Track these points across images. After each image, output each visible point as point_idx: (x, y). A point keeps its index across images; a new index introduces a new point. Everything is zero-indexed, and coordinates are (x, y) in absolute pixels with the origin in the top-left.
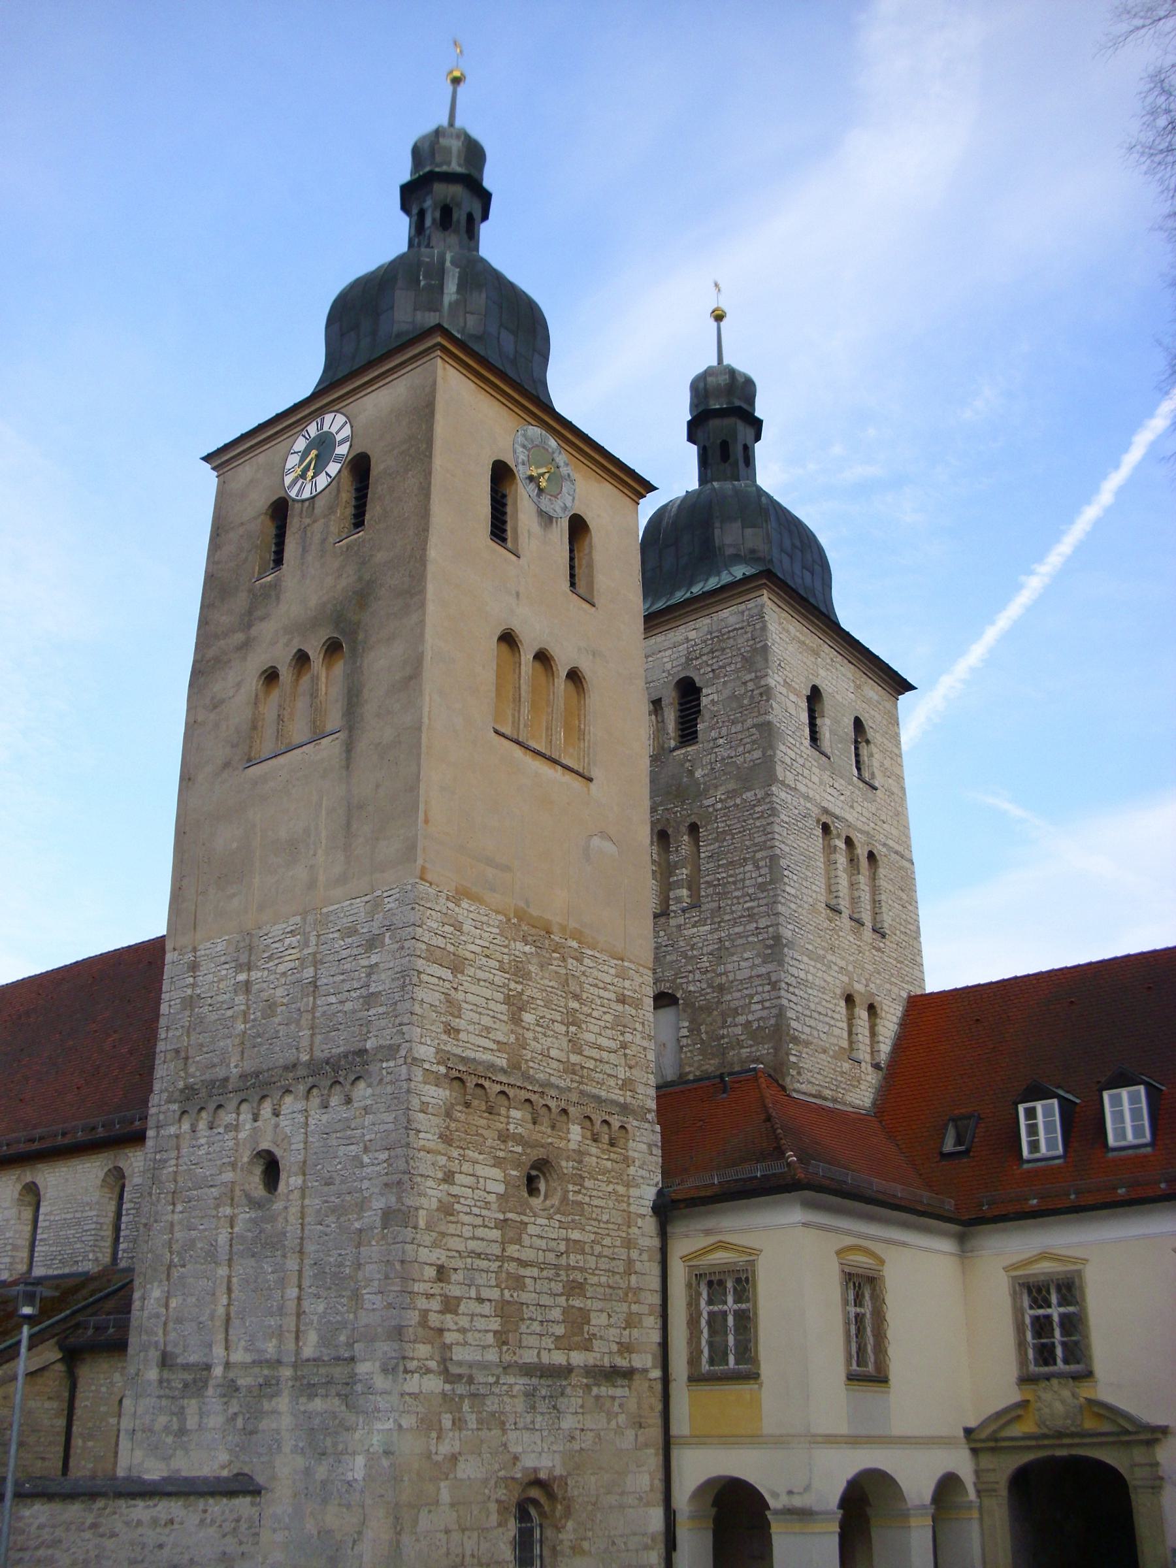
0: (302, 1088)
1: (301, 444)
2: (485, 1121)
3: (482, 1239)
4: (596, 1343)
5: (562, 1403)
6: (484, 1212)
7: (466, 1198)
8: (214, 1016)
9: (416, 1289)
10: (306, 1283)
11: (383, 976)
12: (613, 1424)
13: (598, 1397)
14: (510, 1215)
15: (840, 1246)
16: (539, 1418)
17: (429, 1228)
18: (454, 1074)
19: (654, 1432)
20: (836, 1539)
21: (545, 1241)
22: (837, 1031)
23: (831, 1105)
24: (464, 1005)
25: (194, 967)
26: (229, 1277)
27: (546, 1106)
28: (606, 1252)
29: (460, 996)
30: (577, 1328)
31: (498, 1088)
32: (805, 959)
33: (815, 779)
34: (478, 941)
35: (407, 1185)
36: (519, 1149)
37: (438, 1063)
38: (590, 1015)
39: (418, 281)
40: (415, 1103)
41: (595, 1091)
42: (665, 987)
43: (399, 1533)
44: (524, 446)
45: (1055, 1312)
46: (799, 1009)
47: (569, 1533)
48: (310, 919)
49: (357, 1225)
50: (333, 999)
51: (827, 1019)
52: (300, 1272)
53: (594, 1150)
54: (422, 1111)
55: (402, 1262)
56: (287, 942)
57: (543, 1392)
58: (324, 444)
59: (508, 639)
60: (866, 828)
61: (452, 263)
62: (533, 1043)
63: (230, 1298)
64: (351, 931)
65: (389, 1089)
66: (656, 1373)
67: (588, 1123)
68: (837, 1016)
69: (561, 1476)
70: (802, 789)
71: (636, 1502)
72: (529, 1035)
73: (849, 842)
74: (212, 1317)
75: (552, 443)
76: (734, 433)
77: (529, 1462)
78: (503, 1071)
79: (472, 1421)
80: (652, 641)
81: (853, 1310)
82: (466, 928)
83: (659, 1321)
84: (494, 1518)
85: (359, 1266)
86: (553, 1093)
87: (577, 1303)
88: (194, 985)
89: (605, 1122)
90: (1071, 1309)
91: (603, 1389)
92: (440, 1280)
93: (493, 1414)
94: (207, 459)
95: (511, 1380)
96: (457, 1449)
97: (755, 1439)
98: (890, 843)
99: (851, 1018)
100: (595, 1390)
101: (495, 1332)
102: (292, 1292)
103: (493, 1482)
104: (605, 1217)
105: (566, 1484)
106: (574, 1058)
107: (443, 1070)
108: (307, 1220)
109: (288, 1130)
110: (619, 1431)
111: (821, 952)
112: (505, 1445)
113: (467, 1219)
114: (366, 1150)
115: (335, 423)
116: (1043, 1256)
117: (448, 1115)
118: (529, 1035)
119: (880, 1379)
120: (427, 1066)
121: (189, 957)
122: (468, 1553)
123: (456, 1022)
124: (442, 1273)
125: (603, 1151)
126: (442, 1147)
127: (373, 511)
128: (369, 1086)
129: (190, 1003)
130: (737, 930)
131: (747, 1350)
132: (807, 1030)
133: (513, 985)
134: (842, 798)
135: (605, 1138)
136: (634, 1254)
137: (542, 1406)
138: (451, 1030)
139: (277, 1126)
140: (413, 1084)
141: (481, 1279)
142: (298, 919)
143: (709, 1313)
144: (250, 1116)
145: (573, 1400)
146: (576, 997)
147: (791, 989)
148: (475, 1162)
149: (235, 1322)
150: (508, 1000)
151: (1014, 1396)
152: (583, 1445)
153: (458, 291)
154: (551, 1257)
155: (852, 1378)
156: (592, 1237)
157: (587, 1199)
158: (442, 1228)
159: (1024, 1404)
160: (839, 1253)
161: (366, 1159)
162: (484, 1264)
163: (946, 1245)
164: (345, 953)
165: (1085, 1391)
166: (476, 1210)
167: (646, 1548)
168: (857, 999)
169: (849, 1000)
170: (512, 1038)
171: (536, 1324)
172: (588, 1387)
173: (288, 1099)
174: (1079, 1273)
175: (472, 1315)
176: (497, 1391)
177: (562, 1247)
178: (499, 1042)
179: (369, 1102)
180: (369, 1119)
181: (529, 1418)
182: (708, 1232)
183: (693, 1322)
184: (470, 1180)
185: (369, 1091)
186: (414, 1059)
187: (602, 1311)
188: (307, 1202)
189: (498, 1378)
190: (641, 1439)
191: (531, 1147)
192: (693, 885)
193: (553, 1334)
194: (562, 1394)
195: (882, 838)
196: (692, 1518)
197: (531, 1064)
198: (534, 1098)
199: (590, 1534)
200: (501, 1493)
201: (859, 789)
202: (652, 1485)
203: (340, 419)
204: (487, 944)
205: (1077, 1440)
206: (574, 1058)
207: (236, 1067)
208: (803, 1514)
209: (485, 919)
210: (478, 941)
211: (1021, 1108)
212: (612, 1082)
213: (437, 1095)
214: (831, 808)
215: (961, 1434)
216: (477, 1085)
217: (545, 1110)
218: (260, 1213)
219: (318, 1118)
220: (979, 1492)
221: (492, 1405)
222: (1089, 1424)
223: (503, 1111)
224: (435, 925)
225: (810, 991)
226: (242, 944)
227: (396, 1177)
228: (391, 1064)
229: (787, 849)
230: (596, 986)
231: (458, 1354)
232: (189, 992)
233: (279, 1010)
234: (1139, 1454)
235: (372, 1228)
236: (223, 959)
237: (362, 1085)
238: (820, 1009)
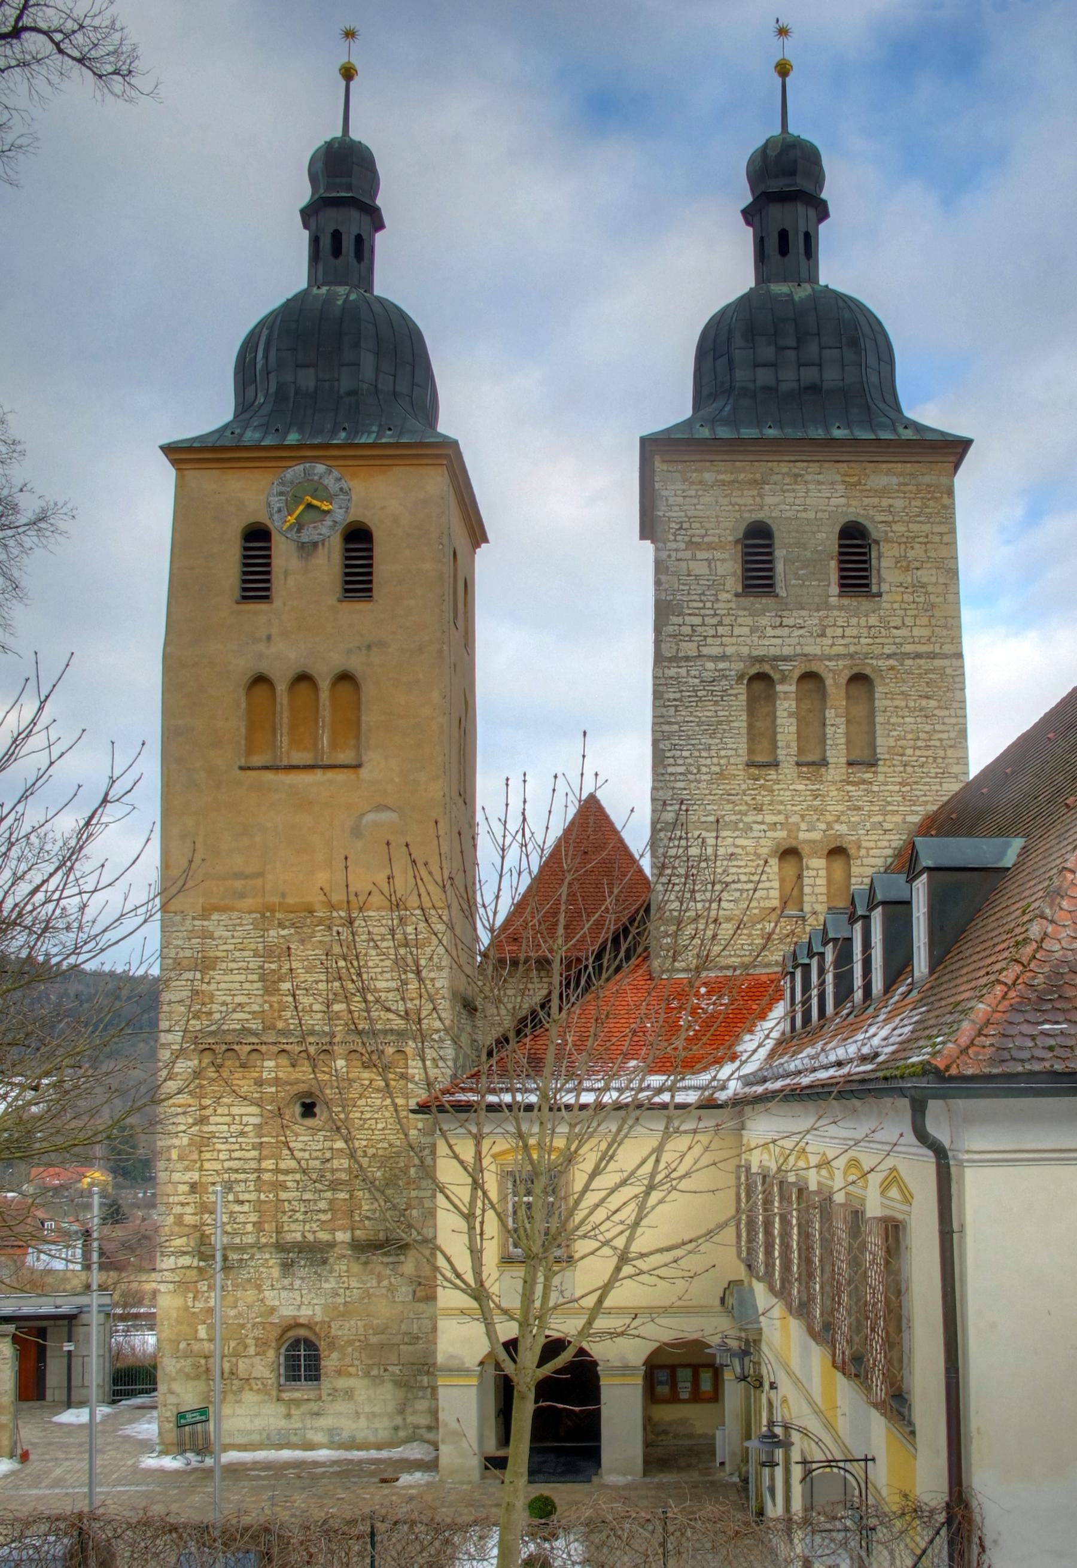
2: (240, 1075)
3: (240, 1159)
6: (240, 1140)
7: (221, 1133)
9: (171, 1201)
12: (385, 1283)
17: (181, 1158)
21: (307, 1153)
36: (273, 1089)
51: (739, 886)
69: (323, 1322)
77: (288, 1311)
82: (216, 935)
84: (252, 1350)
92: (195, 1193)
93: (249, 1280)
98: (908, 648)
101: (254, 1224)
103: (249, 1326)
104: (380, 1126)
105: (330, 1327)
112: (262, 1300)
113: (223, 1147)
124: (194, 1187)
150: (262, 979)
152: (348, 1299)
156: (364, 1143)
162: (242, 1176)
166: (233, 1140)
170: (266, 1007)
171: (298, 1214)
178: (254, 1012)
181: (286, 1282)
184: (228, 1119)
193: (318, 1220)
197: (291, 1021)
198: (288, 1047)
223: (259, 1063)
224: (180, 942)
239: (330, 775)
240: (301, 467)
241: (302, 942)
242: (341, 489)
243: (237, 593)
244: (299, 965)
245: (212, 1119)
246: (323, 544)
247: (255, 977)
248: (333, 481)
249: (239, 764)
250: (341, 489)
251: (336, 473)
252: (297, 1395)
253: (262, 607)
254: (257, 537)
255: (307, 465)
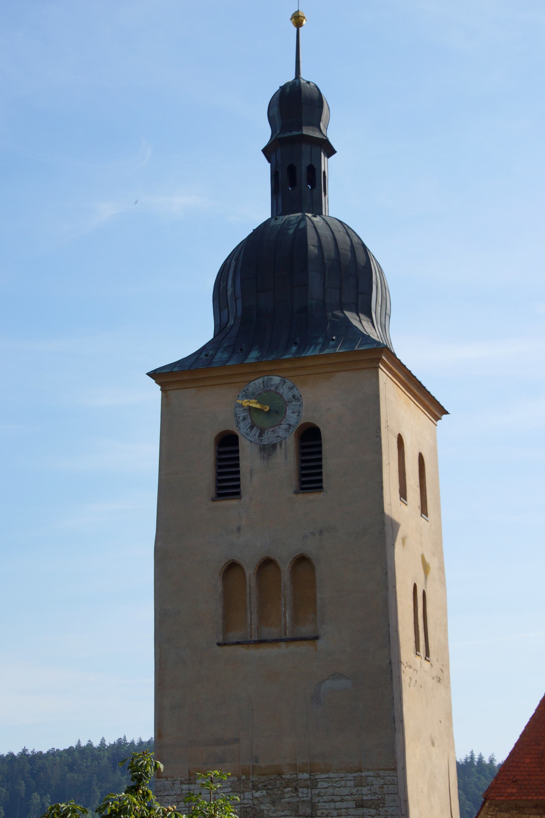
230: (332, 801)
239: (293, 647)
240: (261, 380)
241: (273, 803)
242: (294, 396)
243: (212, 491)
246: (281, 445)
248: (286, 390)
249: (217, 641)
250: (294, 396)
251: (289, 383)
253: (233, 502)
254: (227, 443)
255: (265, 378)
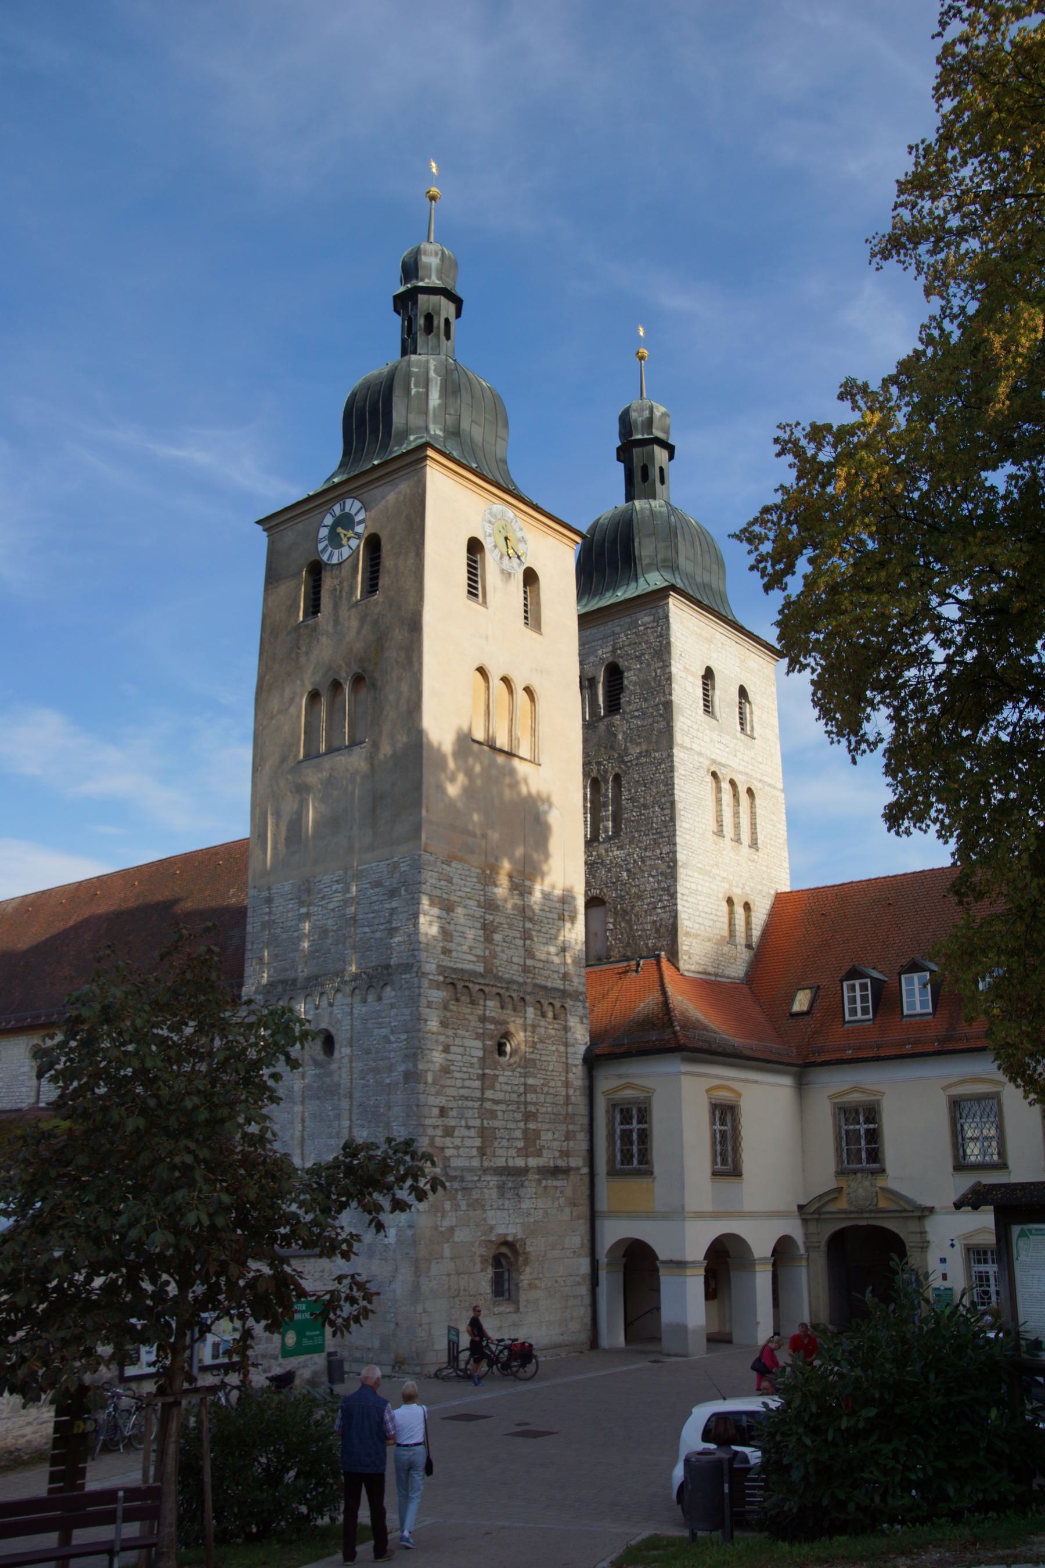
0: (348, 989)
1: (329, 520)
4: (545, 1152)
5: (522, 1192)
6: (470, 1070)
8: (285, 936)
10: (354, 1117)
11: (401, 917)
13: (546, 1187)
14: (487, 1071)
15: (708, 1087)
16: (507, 1202)
17: (434, 1083)
18: (449, 980)
19: (584, 1209)
20: (702, 1279)
22: (719, 925)
23: (713, 978)
24: (455, 933)
25: (269, 900)
26: (303, 1112)
27: (510, 996)
28: (552, 1091)
29: (452, 927)
30: (531, 1142)
31: (478, 987)
32: (696, 875)
33: (707, 739)
34: (463, 889)
35: (420, 1057)
36: (492, 1027)
37: (439, 974)
38: (540, 931)
39: (409, 390)
40: (423, 1001)
41: (543, 983)
42: (595, 892)
43: (418, 1277)
44: (490, 522)
45: (862, 1128)
46: (691, 911)
47: (526, 1277)
48: (350, 872)
49: (388, 1081)
50: (367, 929)
51: (711, 917)
52: (350, 1110)
53: (543, 1023)
54: (428, 1007)
55: (418, 1106)
56: (334, 888)
57: (510, 1185)
58: (346, 521)
59: (481, 670)
60: (747, 770)
61: (435, 371)
62: (501, 954)
63: (303, 1126)
64: (378, 884)
65: (407, 993)
66: (585, 1170)
67: (538, 1006)
68: (719, 913)
70: (696, 747)
71: (572, 1255)
72: (498, 949)
73: (732, 783)
74: (292, 1137)
75: (510, 513)
76: (652, 456)
77: (501, 1230)
78: (481, 975)
79: (463, 1205)
80: (588, 633)
81: (718, 1127)
82: (455, 881)
83: (588, 1135)
85: (390, 1108)
86: (515, 987)
87: (532, 1126)
88: (270, 913)
89: (551, 1004)
90: (872, 1126)
91: (549, 1182)
93: (477, 1200)
94: (259, 522)
95: (489, 1178)
96: (454, 1224)
97: (650, 1215)
98: (765, 779)
99: (731, 913)
100: (544, 1183)
101: (478, 1148)
102: (346, 1123)
104: (551, 1068)
106: (529, 962)
107: (441, 978)
108: (355, 1076)
109: (339, 1016)
110: (560, 1209)
111: (708, 868)
112: (485, 1220)
114: (392, 1032)
115: (352, 506)
116: (854, 1090)
117: (446, 1008)
118: (498, 949)
119: (736, 1173)
120: (431, 977)
121: (266, 894)
122: (462, 1288)
123: (449, 946)
124: (443, 1112)
125: (549, 1023)
126: (441, 1030)
127: (384, 581)
128: (393, 989)
129: (268, 925)
130: (647, 854)
131: (645, 1156)
132: (697, 926)
133: (487, 917)
134: (727, 750)
135: (550, 1014)
136: (571, 1092)
137: (509, 1194)
138: (446, 951)
139: (332, 1012)
140: (422, 990)
141: (469, 1114)
142: (341, 872)
143: (622, 1131)
144: (312, 1006)
145: (530, 1189)
146: (531, 920)
147: (685, 898)
148: (463, 1038)
149: (308, 1142)
150: (484, 927)
151: (834, 1185)
153: (440, 397)
154: (514, 1096)
155: (715, 1174)
156: (542, 1081)
157: (538, 1057)
158: (443, 1082)
159: (840, 1190)
160: (707, 1091)
161: (392, 1038)
162: (470, 1104)
163: (787, 1081)
164: (375, 898)
165: (880, 1183)
166: (464, 1069)
167: (579, 1284)
168: (735, 900)
169: (730, 901)
170: (487, 953)
172: (539, 1181)
173: (339, 996)
174: (878, 1102)
175: (463, 1137)
176: (479, 1185)
177: (522, 1090)
178: (478, 956)
179: (393, 1001)
180: (394, 1012)
181: (500, 1202)
182: (620, 1076)
183: (611, 1135)
184: (460, 1050)
185: (393, 993)
186: (423, 973)
187: (548, 1130)
188: (354, 1065)
189: (480, 1177)
190: (575, 1214)
191: (501, 1024)
192: (616, 818)
194: (522, 1186)
195: (759, 777)
196: (609, 1264)
198: (502, 991)
199: (541, 1276)
200: (482, 1251)
201: (741, 740)
202: (582, 1243)
203: (358, 505)
204: (469, 890)
205: (873, 1215)
206: (529, 962)
207: (302, 971)
208: (681, 1265)
209: (468, 873)
210: (463, 889)
211: (845, 984)
212: (555, 976)
213: (437, 995)
214: (719, 759)
215: (796, 1209)
216: (465, 987)
217: (508, 1000)
218: (322, 1071)
219: (359, 1009)
220: (807, 1249)
221: (476, 1194)
222: (883, 1204)
223: (481, 1002)
224: (434, 881)
225: (699, 898)
226: (303, 888)
227: (413, 1051)
228: (408, 976)
229: (683, 795)
231: (455, 1163)
232: (267, 918)
233: (330, 934)
234: (913, 1226)
235: (397, 1084)
236: (290, 896)
237: (388, 989)
238: (707, 910)
244: (504, 921)
245: (453, 1049)
247: (478, 925)
252: (502, 1309)
